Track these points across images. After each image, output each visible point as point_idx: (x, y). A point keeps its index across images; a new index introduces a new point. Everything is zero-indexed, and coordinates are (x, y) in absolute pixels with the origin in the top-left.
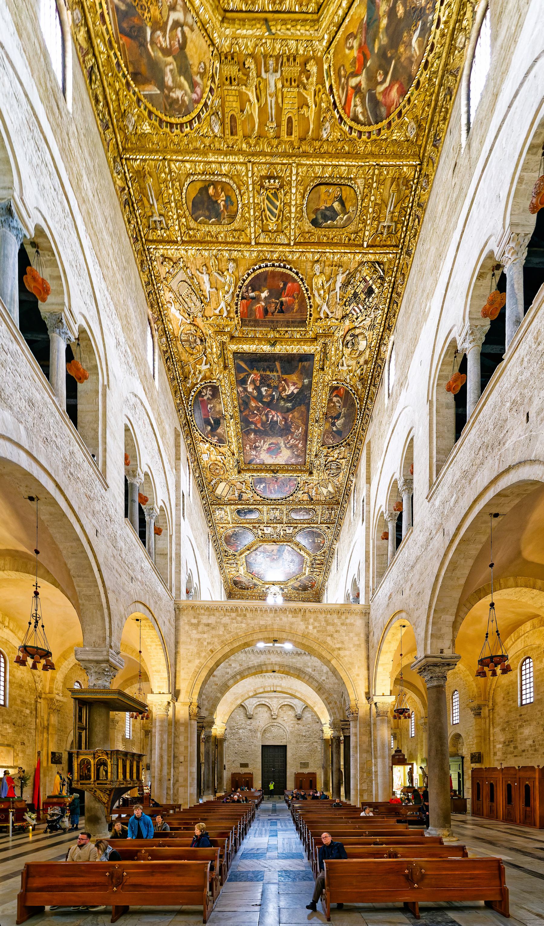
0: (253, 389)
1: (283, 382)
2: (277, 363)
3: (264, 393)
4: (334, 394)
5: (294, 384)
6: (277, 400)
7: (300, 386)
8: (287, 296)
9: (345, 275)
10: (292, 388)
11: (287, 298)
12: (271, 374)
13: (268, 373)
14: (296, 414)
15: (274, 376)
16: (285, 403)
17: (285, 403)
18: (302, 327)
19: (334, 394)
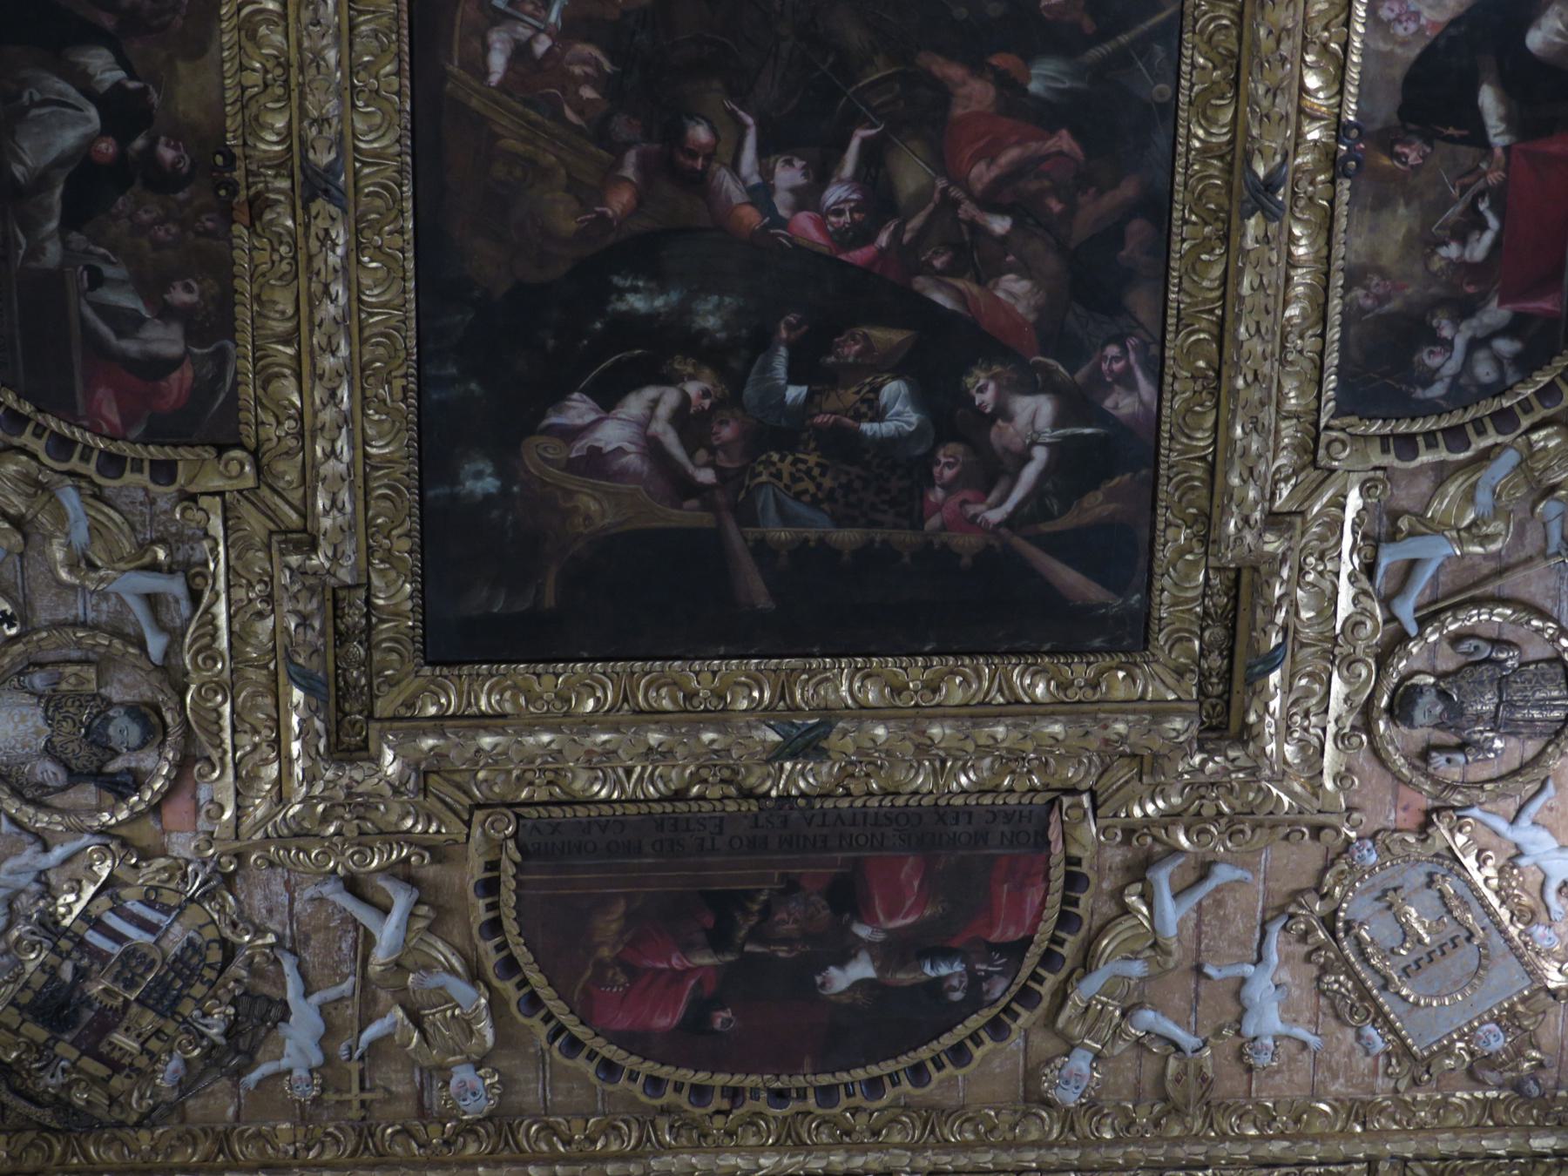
0: (1003, 412)
1: (706, 476)
2: (764, 602)
3: (893, 390)
4: (178, 383)
5: (597, 463)
6: (762, 343)
7: (538, 454)
8: (687, 971)
9: (266, 1069)
10: (613, 434)
11: (676, 962)
12: (819, 528)
13: (847, 537)
14: (566, 219)
15: (786, 519)
16: (683, 311)
17: (683, 311)
18: (556, 827)
19: (178, 383)
